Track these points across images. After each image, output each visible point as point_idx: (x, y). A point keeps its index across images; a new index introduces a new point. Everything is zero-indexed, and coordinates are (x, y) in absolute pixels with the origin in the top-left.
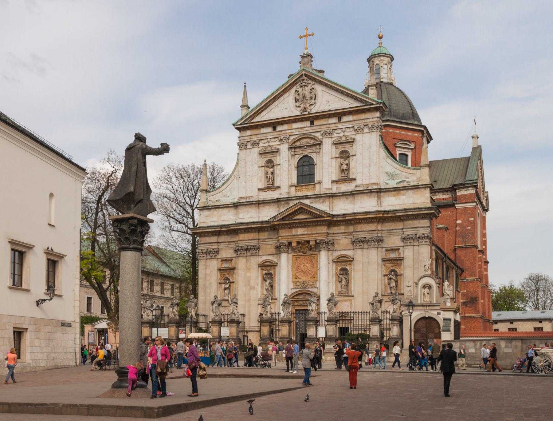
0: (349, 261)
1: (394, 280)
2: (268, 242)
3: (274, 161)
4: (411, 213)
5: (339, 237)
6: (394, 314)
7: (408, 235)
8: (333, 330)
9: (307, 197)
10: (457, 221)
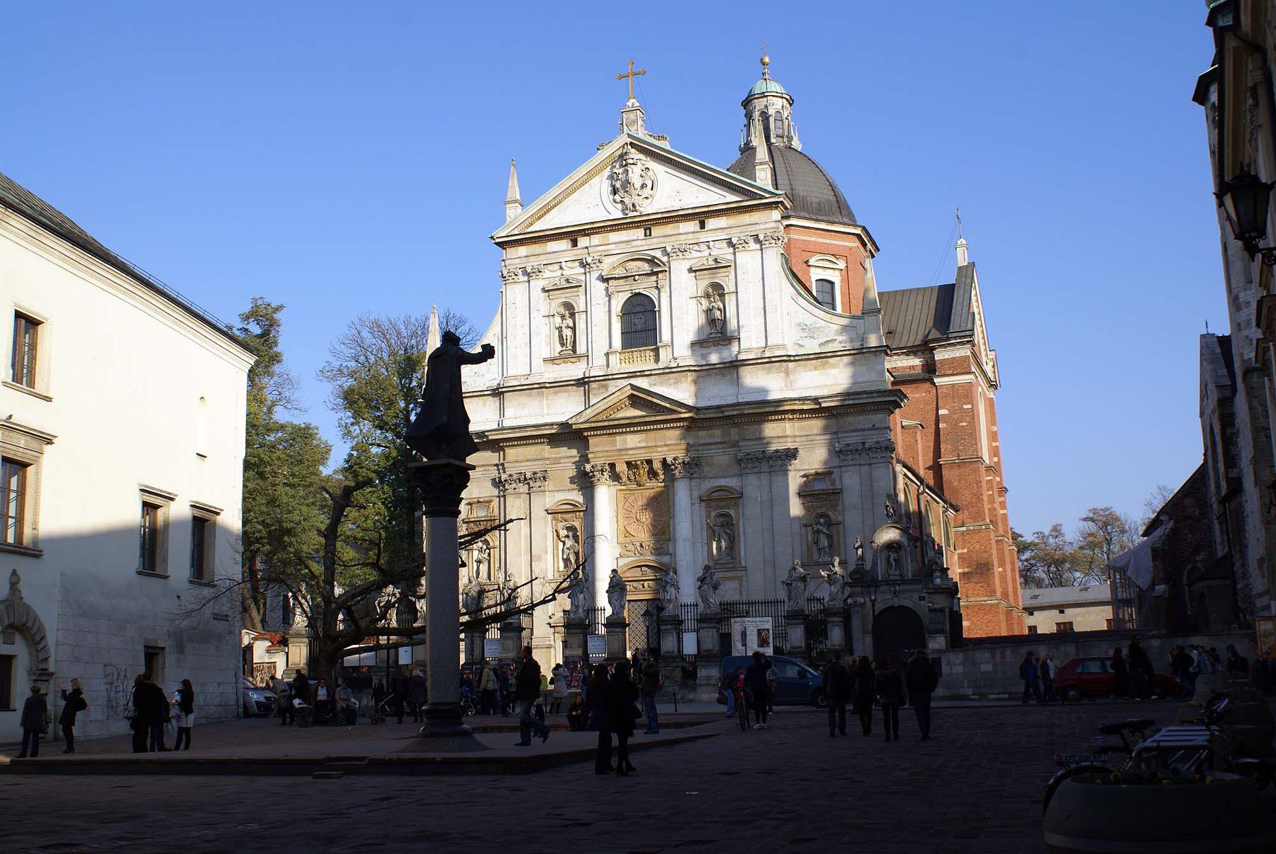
0: (733, 498)
1: (825, 533)
2: (566, 465)
3: (574, 304)
5: (712, 451)
6: (832, 603)
7: (848, 445)
8: (711, 640)
9: (642, 374)
10: (940, 411)
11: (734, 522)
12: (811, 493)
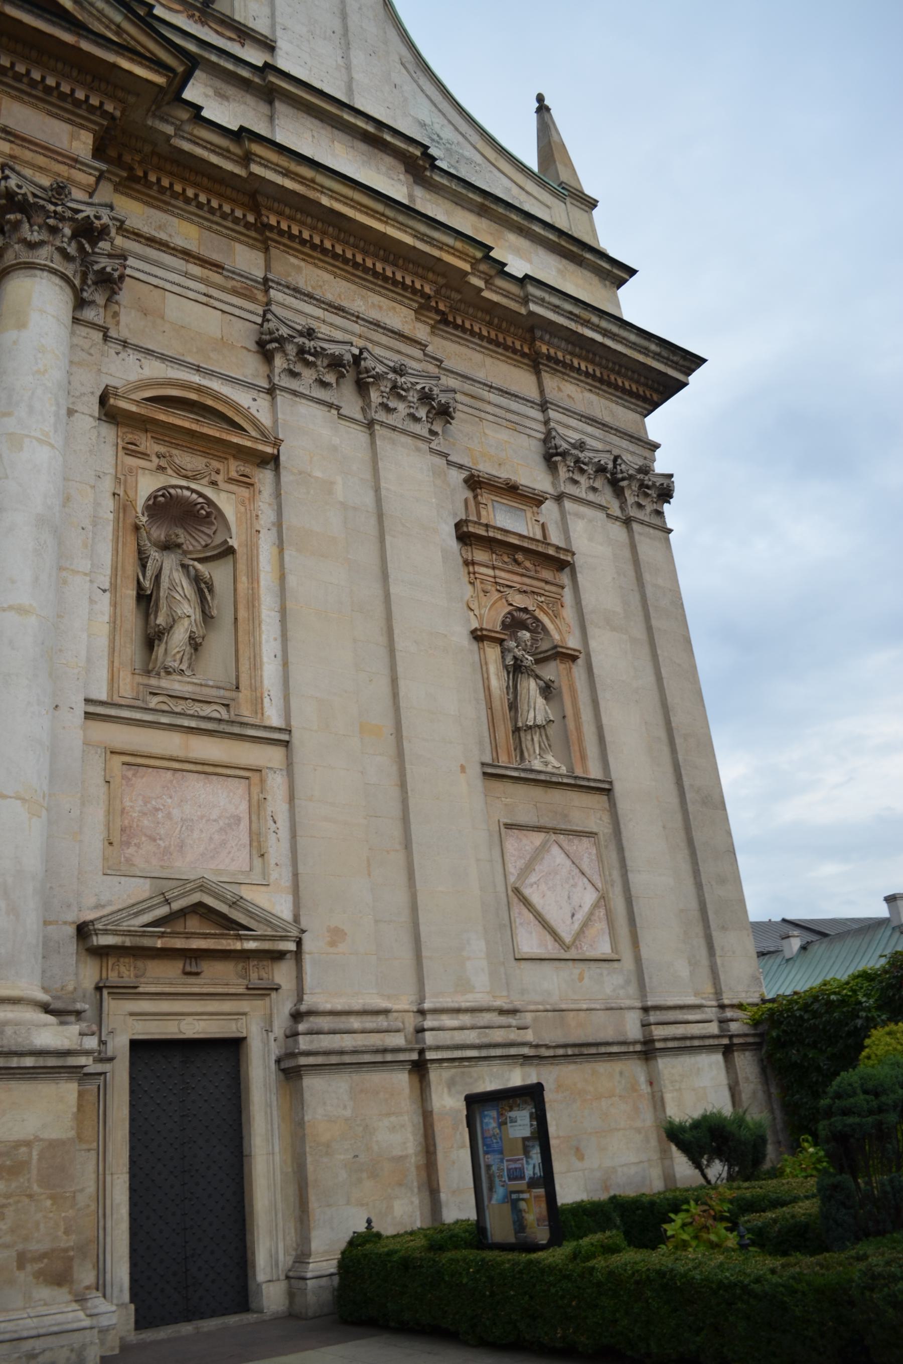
1: (537, 677)
4: (598, 338)
11: (234, 542)
12: (499, 536)
